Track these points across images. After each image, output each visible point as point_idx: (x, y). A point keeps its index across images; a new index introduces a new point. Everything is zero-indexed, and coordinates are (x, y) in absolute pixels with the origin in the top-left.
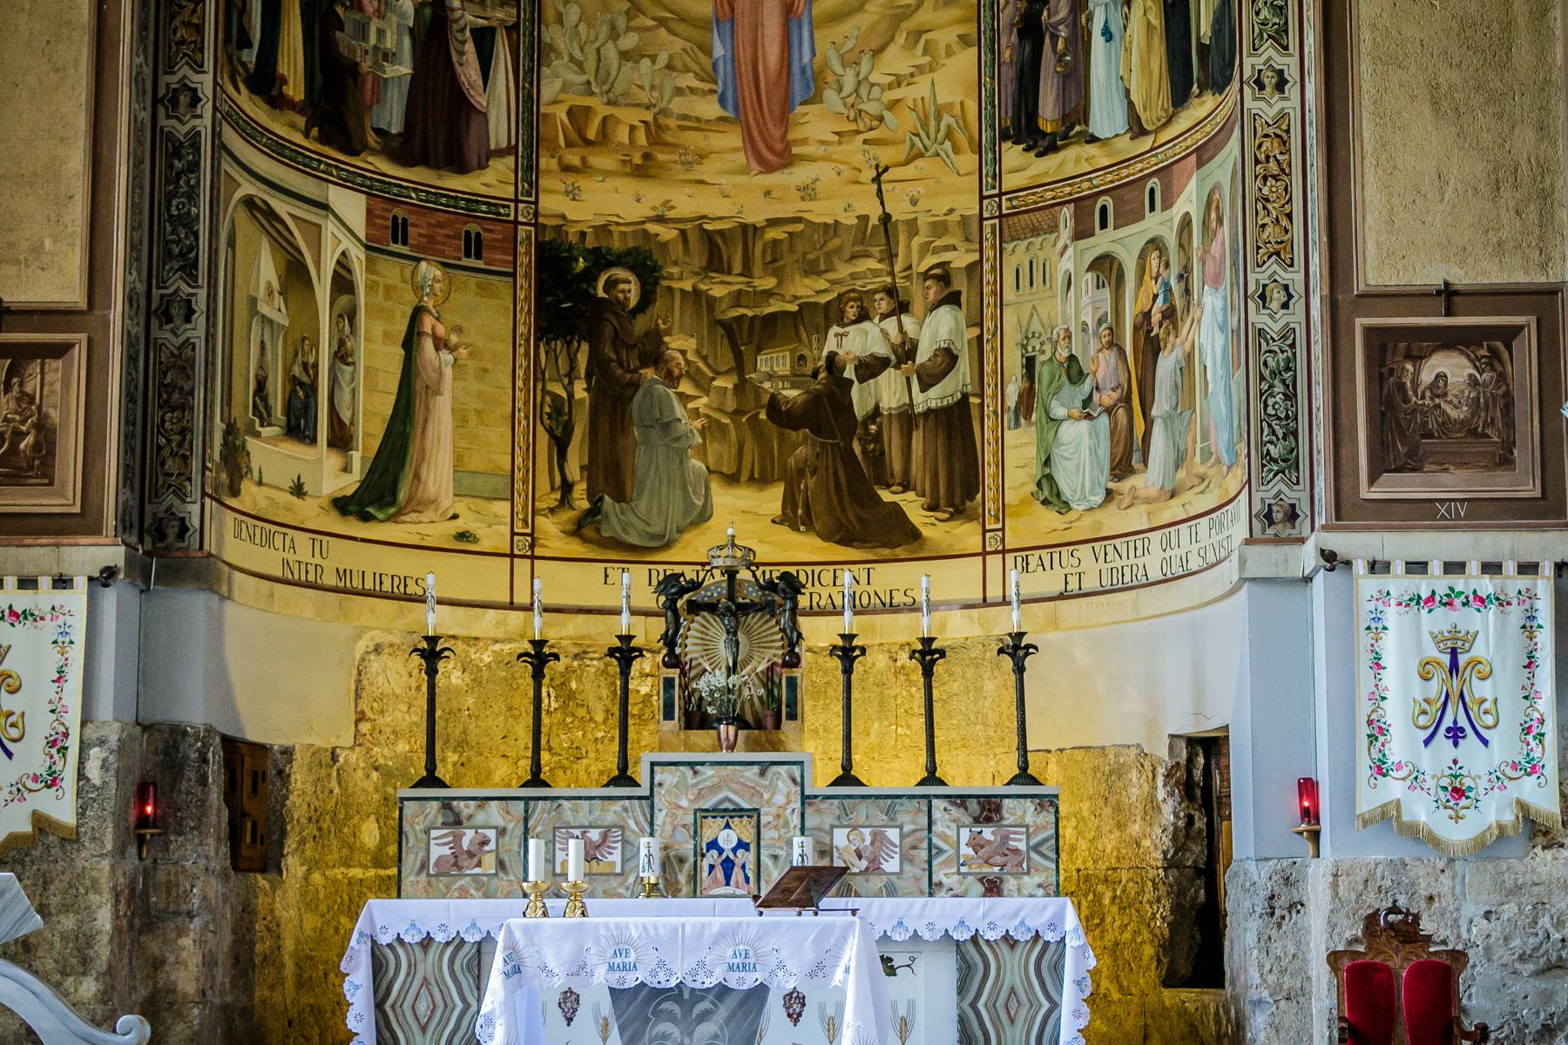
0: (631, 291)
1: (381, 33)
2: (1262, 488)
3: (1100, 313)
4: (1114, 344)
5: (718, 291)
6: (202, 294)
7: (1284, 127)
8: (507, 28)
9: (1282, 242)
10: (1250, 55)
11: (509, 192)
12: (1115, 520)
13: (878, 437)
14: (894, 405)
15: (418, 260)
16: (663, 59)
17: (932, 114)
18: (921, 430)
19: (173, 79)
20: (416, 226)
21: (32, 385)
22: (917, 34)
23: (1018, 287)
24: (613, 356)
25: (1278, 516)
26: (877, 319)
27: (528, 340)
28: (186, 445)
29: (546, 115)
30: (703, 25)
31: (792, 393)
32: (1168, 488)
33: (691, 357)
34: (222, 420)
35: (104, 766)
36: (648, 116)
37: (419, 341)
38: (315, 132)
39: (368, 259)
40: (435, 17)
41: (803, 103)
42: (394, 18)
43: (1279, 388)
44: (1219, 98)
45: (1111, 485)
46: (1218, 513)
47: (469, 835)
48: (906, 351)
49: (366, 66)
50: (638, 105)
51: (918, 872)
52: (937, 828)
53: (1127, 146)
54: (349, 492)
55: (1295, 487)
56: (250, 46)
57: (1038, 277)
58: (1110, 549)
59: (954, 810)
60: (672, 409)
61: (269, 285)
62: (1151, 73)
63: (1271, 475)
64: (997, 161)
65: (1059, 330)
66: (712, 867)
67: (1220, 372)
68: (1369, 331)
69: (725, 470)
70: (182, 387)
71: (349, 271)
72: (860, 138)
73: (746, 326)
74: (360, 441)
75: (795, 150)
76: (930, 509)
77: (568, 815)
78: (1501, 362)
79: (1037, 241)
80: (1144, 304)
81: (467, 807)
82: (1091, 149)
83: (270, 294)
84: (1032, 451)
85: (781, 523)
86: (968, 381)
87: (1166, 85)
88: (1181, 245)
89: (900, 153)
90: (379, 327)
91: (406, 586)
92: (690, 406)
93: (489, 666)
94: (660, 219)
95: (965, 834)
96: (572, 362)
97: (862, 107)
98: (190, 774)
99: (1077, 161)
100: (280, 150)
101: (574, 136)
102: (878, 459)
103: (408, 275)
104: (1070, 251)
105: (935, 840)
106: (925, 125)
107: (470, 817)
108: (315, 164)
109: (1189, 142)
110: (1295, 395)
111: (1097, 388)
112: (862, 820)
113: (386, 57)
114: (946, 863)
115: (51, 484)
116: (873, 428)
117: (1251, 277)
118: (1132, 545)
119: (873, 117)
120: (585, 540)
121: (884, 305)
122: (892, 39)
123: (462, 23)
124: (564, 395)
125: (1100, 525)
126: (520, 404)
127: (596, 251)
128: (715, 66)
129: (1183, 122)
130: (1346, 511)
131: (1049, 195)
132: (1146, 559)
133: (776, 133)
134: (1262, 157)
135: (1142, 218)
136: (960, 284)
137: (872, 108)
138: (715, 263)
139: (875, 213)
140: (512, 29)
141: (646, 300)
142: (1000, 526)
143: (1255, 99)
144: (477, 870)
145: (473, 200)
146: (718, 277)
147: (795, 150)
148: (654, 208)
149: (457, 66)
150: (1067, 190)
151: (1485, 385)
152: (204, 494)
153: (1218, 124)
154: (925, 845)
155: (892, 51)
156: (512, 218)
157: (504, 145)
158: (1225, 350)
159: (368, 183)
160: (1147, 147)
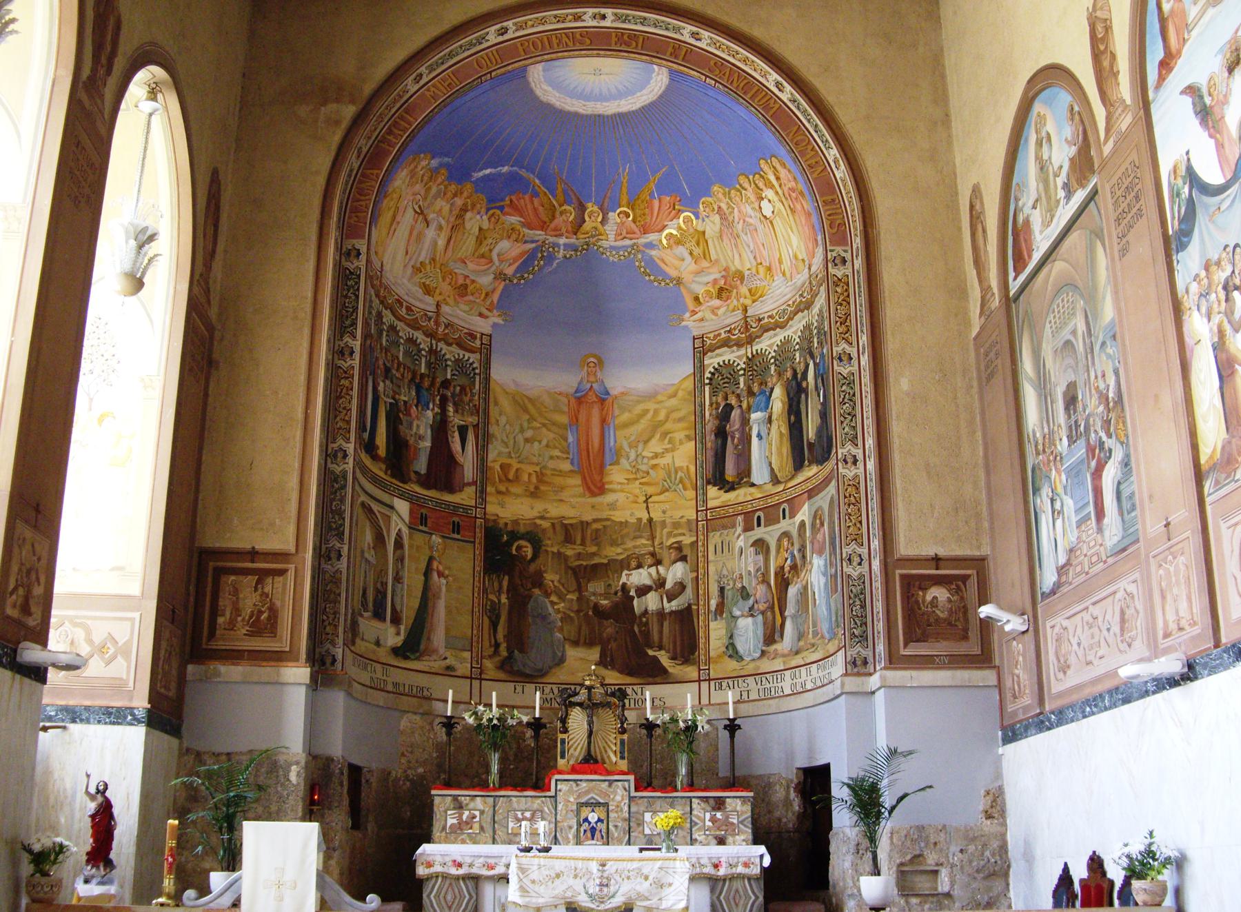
0: (529, 551)
1: (418, 426)
4: (765, 581)
5: (569, 553)
6: (346, 548)
12: (766, 665)
13: (647, 624)
15: (431, 534)
16: (544, 442)
17: (671, 472)
19: (335, 446)
21: (268, 589)
22: (665, 434)
25: (859, 663)
31: (604, 602)
33: (556, 583)
35: (298, 775)
36: (537, 469)
38: (389, 472)
40: (441, 419)
43: (858, 602)
44: (820, 467)
47: (466, 814)
48: (660, 583)
49: (412, 441)
50: (533, 464)
51: (685, 834)
52: (695, 812)
53: (770, 488)
54: (399, 645)
57: (726, 550)
58: (764, 679)
62: (782, 455)
64: (705, 494)
65: (737, 574)
66: (585, 831)
67: (823, 594)
68: (903, 577)
72: (637, 482)
75: (607, 486)
76: (672, 659)
77: (515, 805)
78: (961, 591)
80: (780, 561)
82: (752, 490)
94: (542, 518)
95: (708, 815)
97: (640, 467)
99: (745, 495)
100: (375, 480)
102: (647, 634)
103: (427, 539)
104: (742, 537)
107: (467, 804)
112: (658, 809)
114: (699, 829)
117: (844, 551)
119: (644, 472)
121: (650, 561)
124: (496, 600)
126: (476, 605)
127: (512, 532)
128: (568, 446)
129: (800, 478)
130: (894, 661)
131: (731, 510)
133: (597, 477)
136: (687, 551)
137: (644, 468)
138: (568, 539)
139: (645, 516)
140: (476, 426)
141: (536, 556)
144: (470, 831)
145: (457, 506)
146: (570, 546)
151: (955, 602)
152: (344, 644)
155: (653, 442)
158: (826, 584)
160: (781, 489)
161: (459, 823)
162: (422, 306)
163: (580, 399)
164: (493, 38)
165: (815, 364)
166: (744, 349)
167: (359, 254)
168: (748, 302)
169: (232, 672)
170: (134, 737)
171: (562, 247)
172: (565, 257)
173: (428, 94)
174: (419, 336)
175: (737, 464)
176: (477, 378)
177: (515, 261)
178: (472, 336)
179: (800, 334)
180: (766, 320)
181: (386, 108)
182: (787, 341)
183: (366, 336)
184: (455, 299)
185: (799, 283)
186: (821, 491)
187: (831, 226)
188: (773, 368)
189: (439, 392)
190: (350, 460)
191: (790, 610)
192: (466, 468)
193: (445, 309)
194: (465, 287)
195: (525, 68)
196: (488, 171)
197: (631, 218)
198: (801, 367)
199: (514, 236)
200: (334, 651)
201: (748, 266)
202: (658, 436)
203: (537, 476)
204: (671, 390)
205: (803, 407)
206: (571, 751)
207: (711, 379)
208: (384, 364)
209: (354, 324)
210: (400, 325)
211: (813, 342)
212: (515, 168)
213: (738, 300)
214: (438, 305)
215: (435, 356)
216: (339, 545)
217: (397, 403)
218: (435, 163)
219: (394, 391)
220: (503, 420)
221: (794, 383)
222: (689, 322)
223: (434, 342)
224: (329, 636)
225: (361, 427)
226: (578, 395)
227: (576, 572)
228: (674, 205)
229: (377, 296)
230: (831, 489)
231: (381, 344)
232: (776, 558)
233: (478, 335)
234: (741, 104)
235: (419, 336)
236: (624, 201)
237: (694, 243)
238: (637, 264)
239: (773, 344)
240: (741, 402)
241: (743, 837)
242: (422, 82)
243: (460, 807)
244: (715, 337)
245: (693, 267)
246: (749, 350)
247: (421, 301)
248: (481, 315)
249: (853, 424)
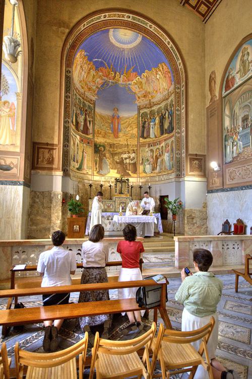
0: (103, 149)
12: (152, 175)
17: (132, 134)
30: (110, 123)
48: (130, 157)
53: (154, 139)
64: (139, 139)
84: (143, 168)
102: (126, 167)
121: (127, 152)
136: (135, 151)
138: (111, 147)
141: (104, 150)
155: (128, 128)
158: (169, 159)
163: (113, 117)
164: (103, 19)
169: (44, 172)
170: (20, 189)
181: (76, 33)
182: (161, 107)
195: (108, 31)
196: (96, 60)
198: (164, 114)
205: (164, 121)
209: (70, 90)
215: (84, 105)
220: (98, 120)
222: (137, 102)
227: (112, 154)
230: (173, 139)
242: (85, 27)
245: (139, 90)
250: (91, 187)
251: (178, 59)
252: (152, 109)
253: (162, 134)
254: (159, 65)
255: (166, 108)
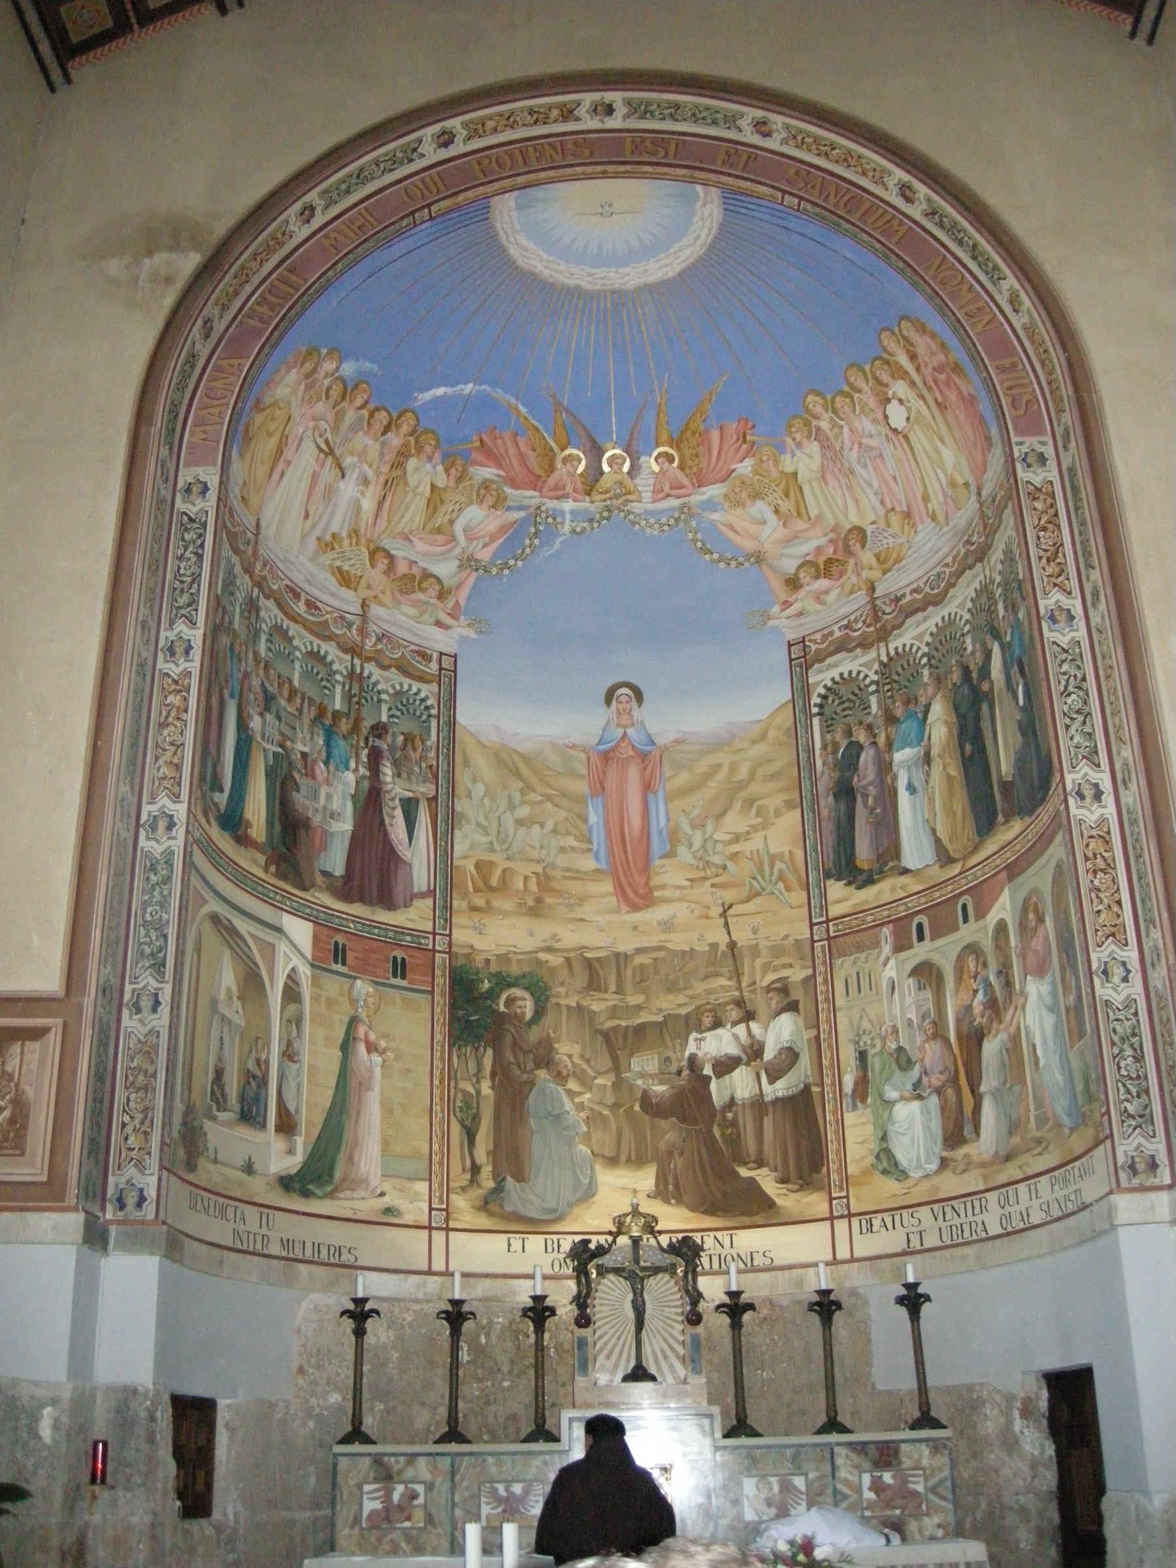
0: (528, 1007)
1: (329, 797)
2: (1125, 1142)
3: (923, 1010)
5: (596, 1006)
6: (168, 989)
7: (1106, 829)
8: (428, 799)
9: (1115, 925)
10: (1070, 772)
11: (429, 927)
12: (950, 1184)
13: (734, 1123)
14: (747, 1095)
15: (355, 978)
16: (549, 826)
18: (771, 1117)
20: (352, 950)
22: (750, 802)
23: (848, 994)
24: (512, 1060)
25: (1141, 1167)
26: (729, 1026)
27: (443, 1047)
28: (147, 1123)
29: (458, 867)
30: (581, 800)
31: (660, 1089)
32: (1002, 1153)
33: (576, 1060)
34: (182, 1101)
37: (355, 1043)
38: (273, 868)
39: (313, 975)
41: (660, 858)
42: (340, 787)
43: (1129, 1052)
44: (1028, 820)
45: (945, 1154)
46: (1062, 1170)
47: (399, 1490)
48: (755, 1051)
49: (316, 820)
50: (532, 860)
52: (842, 1474)
54: (294, 1171)
55: (1153, 1140)
56: (222, 790)
58: (948, 1209)
59: (854, 1456)
60: (563, 1105)
61: (229, 990)
62: (954, 813)
63: (1130, 1130)
64: (823, 894)
69: (607, 1154)
70: (146, 1071)
71: (298, 984)
72: (708, 883)
73: (620, 1035)
74: (303, 1126)
75: (656, 894)
79: (863, 956)
80: (965, 997)
81: (397, 1462)
82: (904, 879)
83: (230, 998)
84: (869, 1129)
85: (655, 1197)
86: (809, 1073)
87: (970, 820)
88: (998, 947)
89: (744, 893)
90: (321, 1033)
91: (340, 1254)
92: (576, 1100)
93: (410, 1325)
94: (549, 950)
95: (867, 1480)
96: (479, 1064)
97: (708, 858)
98: (140, 1431)
99: (893, 889)
100: (242, 878)
101: (480, 884)
102: (735, 1141)
103: (346, 988)
104: (892, 962)
105: (839, 1486)
106: (761, 870)
107: (400, 1472)
108: (272, 895)
109: (998, 862)
110: (1143, 1057)
111: (926, 1073)
113: (332, 815)
115: (22, 1154)
116: (730, 1115)
117: (1094, 957)
118: (969, 1205)
119: (717, 866)
120: (491, 1214)
121: (734, 1014)
122: (730, 807)
123: (393, 793)
125: (937, 1189)
126: (436, 1099)
128: (590, 830)
129: (991, 846)
131: (869, 918)
132: (985, 1216)
134: (1090, 855)
135: (957, 929)
136: (796, 994)
137: (717, 859)
138: (594, 984)
139: (722, 939)
141: (539, 1013)
142: (844, 1194)
143: (1078, 807)
144: (407, 1524)
145: (400, 930)
146: (598, 995)
147: (656, 894)
148: (544, 941)
149: (388, 827)
150: (886, 913)
152: (162, 1167)
153: (1029, 841)
154: (830, 1491)
155: (731, 815)
156: (431, 947)
157: (425, 889)
158: (1057, 1027)
159: (315, 913)
160: (957, 871)
161: (386, 1510)
162: (335, 603)
164: (431, 154)
165: (1004, 647)
166: (874, 649)
167: (205, 489)
168: (875, 574)
171: (568, 516)
172: (574, 531)
173: (326, 242)
174: (331, 650)
175: (876, 841)
176: (434, 723)
177: (493, 540)
178: (425, 656)
179: (969, 605)
180: (908, 598)
183: (217, 628)
184: (394, 598)
185: (963, 523)
186: (1031, 862)
187: (1014, 403)
188: (926, 672)
189: (367, 739)
190: (180, 832)
191: (989, 1082)
192: (415, 867)
193: (376, 611)
194: (409, 577)
196: (440, 391)
197: (675, 464)
199: (490, 500)
200: (140, 1180)
201: (872, 518)
202: (738, 806)
203: (539, 883)
204: (757, 730)
205: (985, 725)
206: (601, 1359)
207: (821, 706)
208: (263, 685)
209: (193, 602)
210: (294, 629)
211: (996, 611)
212: (484, 387)
213: (859, 575)
214: (364, 605)
216: (156, 985)
217: (287, 755)
218: (348, 369)
219: (282, 734)
220: (479, 790)
221: (966, 690)
223: (357, 662)
224: (133, 1154)
225: (208, 779)
226: (601, 747)
227: (607, 1037)
228: (745, 434)
229: (248, 570)
231: (256, 654)
232: (957, 991)
233: (435, 656)
234: (845, 233)
235: (331, 650)
236: (664, 437)
237: (780, 493)
238: (690, 536)
239: (923, 634)
240: (875, 736)
241: (936, 1520)
243: (385, 1475)
244: (824, 638)
245: (782, 532)
246: (883, 651)
247: (333, 595)
248: (438, 624)
249: (1088, 729)
250: (540, 1328)
251: (996, 277)
252: (897, 643)
253: (985, 822)
254: (890, 343)
255: (982, 620)
